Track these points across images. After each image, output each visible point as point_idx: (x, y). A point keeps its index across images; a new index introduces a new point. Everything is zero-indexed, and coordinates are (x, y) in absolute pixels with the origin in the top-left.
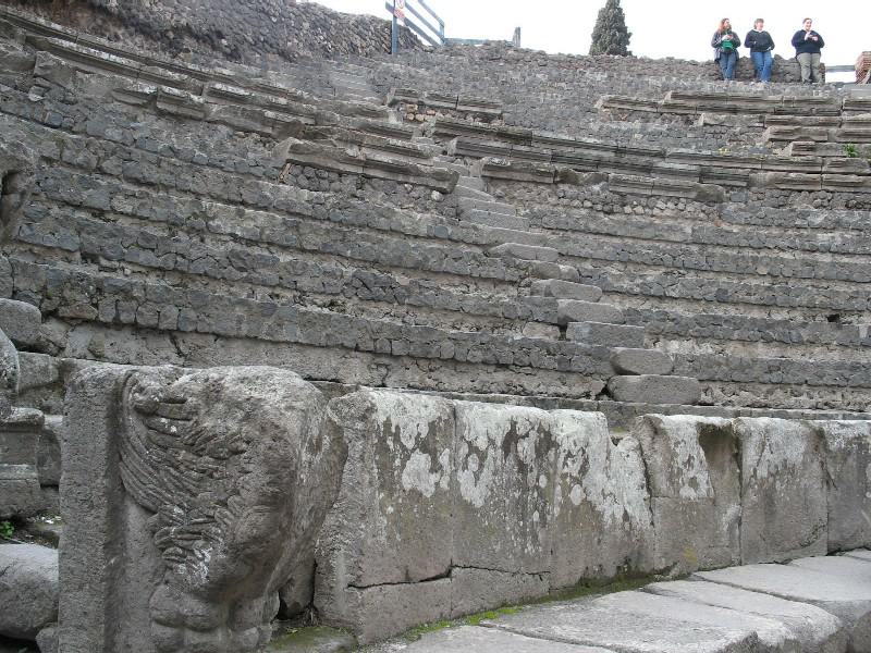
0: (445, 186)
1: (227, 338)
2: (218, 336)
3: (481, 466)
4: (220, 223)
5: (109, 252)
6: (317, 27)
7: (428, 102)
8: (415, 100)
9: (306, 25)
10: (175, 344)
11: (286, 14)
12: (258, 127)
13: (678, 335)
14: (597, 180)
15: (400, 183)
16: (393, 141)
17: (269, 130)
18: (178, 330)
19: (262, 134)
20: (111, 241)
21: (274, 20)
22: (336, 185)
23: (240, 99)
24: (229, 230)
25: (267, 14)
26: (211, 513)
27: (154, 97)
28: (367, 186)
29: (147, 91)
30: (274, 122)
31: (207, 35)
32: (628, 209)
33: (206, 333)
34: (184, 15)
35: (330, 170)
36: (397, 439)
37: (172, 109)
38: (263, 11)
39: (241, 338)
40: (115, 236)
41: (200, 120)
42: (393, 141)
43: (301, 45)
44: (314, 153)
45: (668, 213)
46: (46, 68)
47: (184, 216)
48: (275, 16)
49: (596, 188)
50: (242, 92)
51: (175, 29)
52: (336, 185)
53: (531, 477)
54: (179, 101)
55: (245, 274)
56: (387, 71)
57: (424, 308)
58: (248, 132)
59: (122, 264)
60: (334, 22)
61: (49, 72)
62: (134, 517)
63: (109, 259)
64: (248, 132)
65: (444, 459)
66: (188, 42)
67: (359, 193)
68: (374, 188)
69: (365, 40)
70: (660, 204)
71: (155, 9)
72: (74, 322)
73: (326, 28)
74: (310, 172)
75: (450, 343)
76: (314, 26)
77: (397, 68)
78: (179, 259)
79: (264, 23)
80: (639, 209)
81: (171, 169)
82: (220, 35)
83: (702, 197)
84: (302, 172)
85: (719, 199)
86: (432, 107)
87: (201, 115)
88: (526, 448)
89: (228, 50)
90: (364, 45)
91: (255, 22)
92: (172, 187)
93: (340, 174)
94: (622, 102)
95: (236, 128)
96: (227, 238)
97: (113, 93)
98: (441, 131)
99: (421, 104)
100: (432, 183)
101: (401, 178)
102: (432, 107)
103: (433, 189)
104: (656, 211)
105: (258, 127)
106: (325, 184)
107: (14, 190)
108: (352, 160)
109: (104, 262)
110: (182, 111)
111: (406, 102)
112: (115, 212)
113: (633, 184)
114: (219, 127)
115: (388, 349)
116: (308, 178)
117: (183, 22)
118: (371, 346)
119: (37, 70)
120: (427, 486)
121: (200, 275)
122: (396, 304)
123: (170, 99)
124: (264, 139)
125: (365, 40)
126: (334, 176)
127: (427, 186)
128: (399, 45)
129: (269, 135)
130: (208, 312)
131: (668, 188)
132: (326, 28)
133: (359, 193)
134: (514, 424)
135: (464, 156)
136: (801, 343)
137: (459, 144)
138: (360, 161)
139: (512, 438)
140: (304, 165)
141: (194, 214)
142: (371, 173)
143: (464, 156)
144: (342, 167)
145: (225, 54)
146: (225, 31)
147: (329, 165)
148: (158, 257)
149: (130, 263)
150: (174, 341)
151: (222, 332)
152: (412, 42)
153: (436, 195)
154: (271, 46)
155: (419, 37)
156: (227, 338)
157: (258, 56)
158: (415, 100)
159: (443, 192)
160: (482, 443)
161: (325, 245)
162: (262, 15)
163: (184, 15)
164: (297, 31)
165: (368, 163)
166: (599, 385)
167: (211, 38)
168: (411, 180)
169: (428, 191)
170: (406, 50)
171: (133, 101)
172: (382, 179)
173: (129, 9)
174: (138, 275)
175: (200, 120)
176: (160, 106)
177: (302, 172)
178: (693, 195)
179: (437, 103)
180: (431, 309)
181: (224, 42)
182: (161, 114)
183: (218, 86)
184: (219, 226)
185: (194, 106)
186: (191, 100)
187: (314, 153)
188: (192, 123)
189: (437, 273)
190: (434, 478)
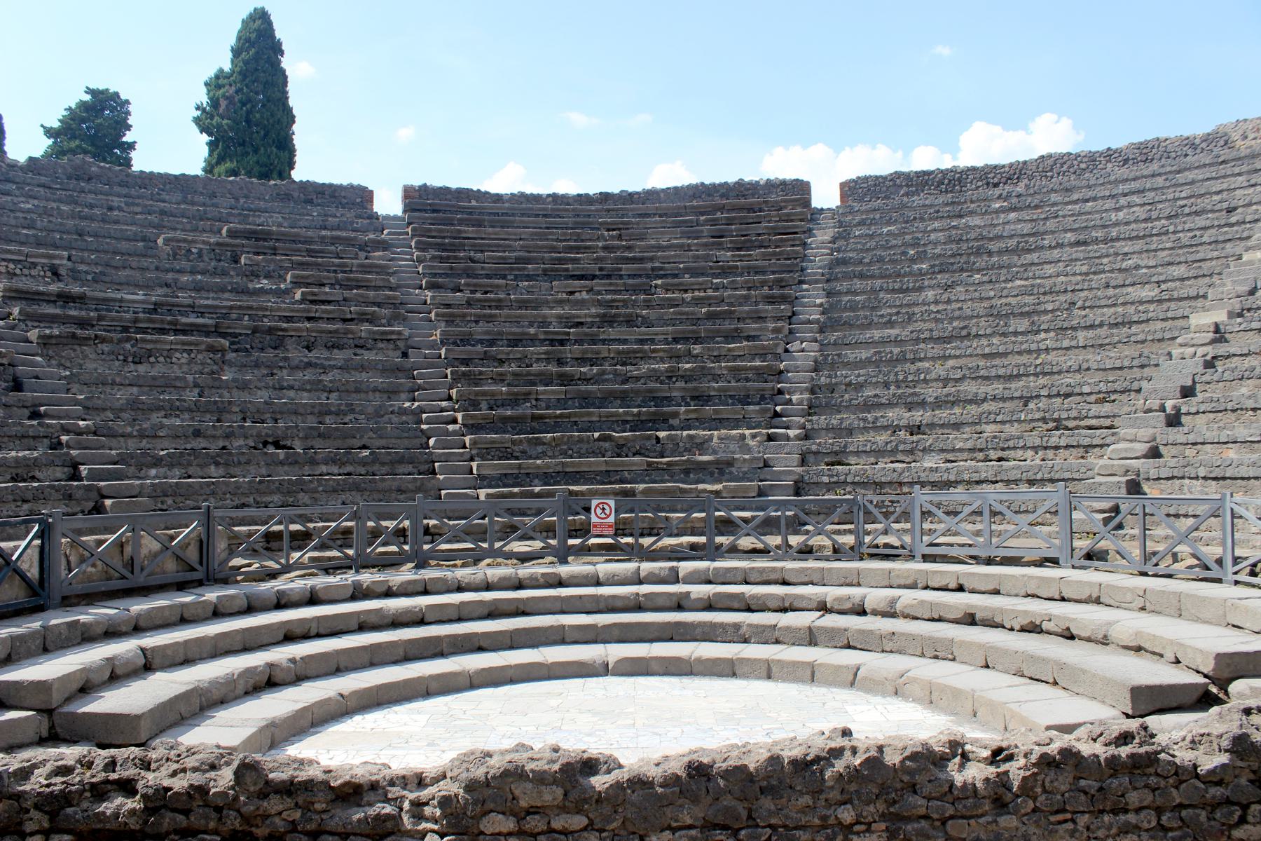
13: (155, 465)
14: (128, 340)
32: (152, 359)
45: (183, 361)
49: (128, 346)
70: (178, 355)
80: (161, 359)
83: (211, 349)
85: (223, 351)
94: (179, 241)
104: (174, 360)
113: (156, 342)
131: (184, 344)
136: (240, 463)
166: (91, 504)
178: (203, 347)
179: (9, 257)
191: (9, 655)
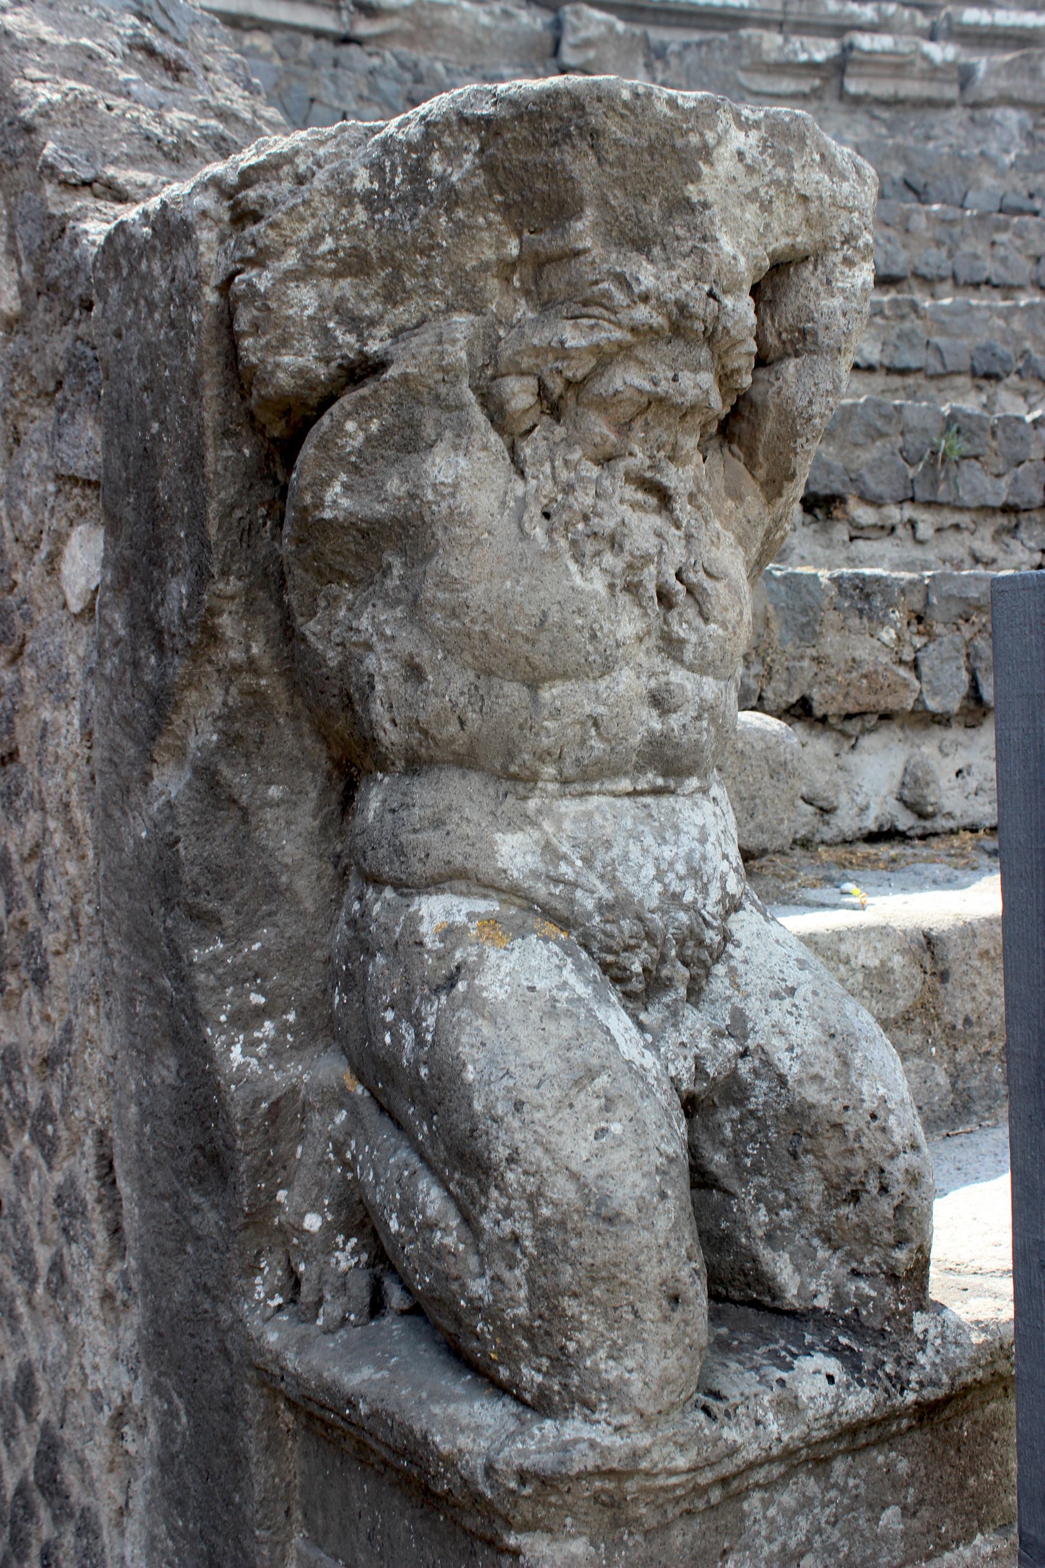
5: (874, 485)
27: (839, 66)
29: (819, 57)
37: (884, 88)
40: (882, 435)
41: (949, 105)
46: (587, 43)
54: (897, 66)
61: (591, 54)
63: (875, 502)
72: (853, 727)
87: (951, 92)
92: (942, 279)
97: (742, 77)
109: (865, 515)
110: (911, 88)
114: (998, 113)
148: (998, 476)
171: (787, 85)
174: (951, 536)
175: (949, 105)
176: (853, 86)
185: (934, 72)
186: (926, 57)
188: (932, 116)
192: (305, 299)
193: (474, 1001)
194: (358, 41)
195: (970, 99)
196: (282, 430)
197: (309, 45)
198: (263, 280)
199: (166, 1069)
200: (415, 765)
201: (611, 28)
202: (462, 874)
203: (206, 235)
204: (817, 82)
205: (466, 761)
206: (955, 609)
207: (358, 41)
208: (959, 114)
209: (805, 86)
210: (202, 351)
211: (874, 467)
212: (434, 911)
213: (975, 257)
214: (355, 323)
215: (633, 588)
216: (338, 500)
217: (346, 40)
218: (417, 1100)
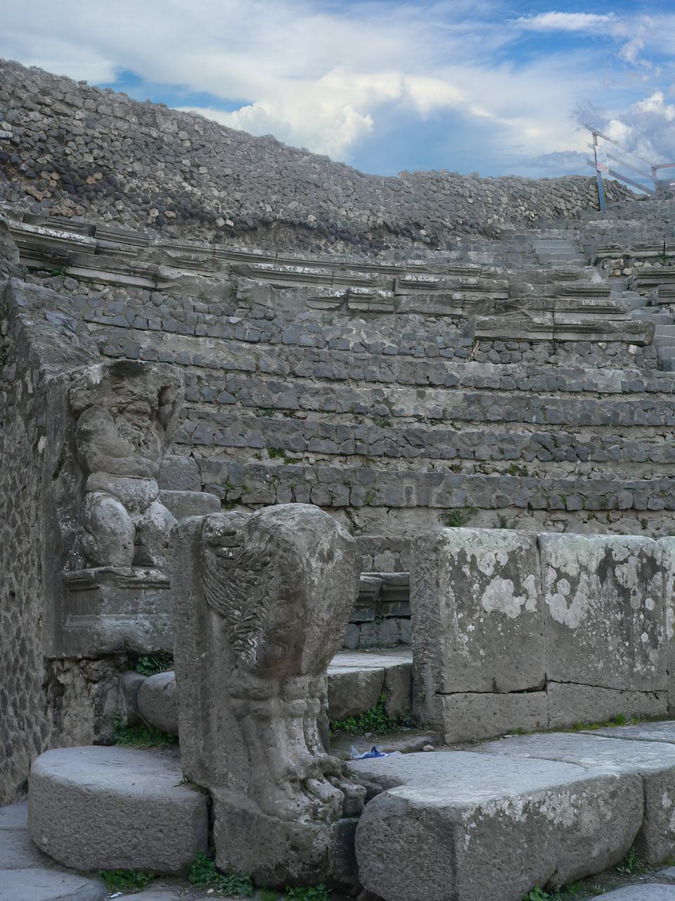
0: (642, 338)
1: (399, 508)
2: (390, 507)
3: (573, 591)
4: (403, 407)
5: (293, 446)
6: (515, 199)
7: (633, 254)
8: (619, 254)
9: (505, 200)
10: (351, 518)
11: (481, 193)
12: (448, 310)
15: (593, 342)
16: (586, 302)
17: (459, 312)
18: (351, 505)
19: (453, 316)
20: (293, 436)
21: (471, 201)
22: (529, 354)
23: (432, 286)
24: (412, 413)
25: (463, 196)
26: (255, 611)
27: (346, 299)
28: (559, 350)
29: (338, 294)
30: (463, 303)
31: (405, 229)
33: (380, 506)
34: (380, 214)
35: (519, 340)
36: (473, 565)
37: (364, 307)
38: (458, 194)
39: (412, 508)
41: (391, 313)
42: (586, 302)
43: (502, 220)
44: (502, 327)
47: (368, 405)
48: (470, 197)
50: (432, 279)
51: (373, 230)
52: (529, 354)
53: (635, 602)
54: (368, 299)
55: (423, 450)
56: (594, 229)
57: (609, 463)
58: (438, 316)
59: (307, 454)
60: (533, 190)
61: (249, 294)
62: (215, 622)
63: (294, 452)
64: (438, 316)
65: (529, 582)
66: (387, 239)
67: (552, 359)
68: (567, 351)
69: (569, 201)
71: (352, 215)
73: (525, 198)
74: (501, 346)
75: (626, 493)
76: (513, 198)
77: (604, 224)
78: (359, 443)
79: (460, 206)
81: (359, 363)
82: (418, 226)
84: (492, 347)
86: (638, 259)
87: (391, 308)
88: (627, 573)
89: (428, 240)
90: (569, 206)
91: (452, 206)
92: (361, 380)
93: (531, 343)
95: (430, 315)
96: (412, 420)
97: (308, 303)
98: (644, 282)
99: (627, 257)
100: (628, 337)
101: (593, 337)
102: (638, 259)
103: (629, 343)
105: (448, 310)
106: (517, 354)
107: (167, 402)
108: (541, 328)
109: (289, 454)
110: (373, 307)
111: (610, 257)
112: (305, 410)
114: (411, 316)
115: (561, 506)
116: (499, 352)
117: (380, 221)
118: (544, 504)
119: (239, 296)
120: (513, 607)
121: (380, 456)
122: (579, 462)
123: (360, 298)
124: (455, 321)
125: (569, 201)
126: (525, 346)
127: (623, 341)
128: (608, 200)
129: (460, 317)
130: (377, 486)
132: (525, 198)
133: (552, 359)
134: (609, 552)
135: (668, 304)
137: (662, 293)
138: (549, 327)
139: (607, 565)
140: (493, 340)
141: (378, 402)
142: (563, 337)
143: (668, 304)
144: (532, 336)
145: (425, 243)
146: (422, 221)
147: (519, 336)
149: (313, 452)
150: (349, 515)
151: (392, 504)
152: (619, 192)
153: (633, 349)
154: (471, 226)
155: (629, 187)
156: (399, 508)
157: (458, 239)
158: (619, 254)
159: (640, 344)
160: (572, 570)
161: (509, 414)
162: (459, 199)
163: (380, 214)
164: (495, 207)
165: (558, 328)
167: (409, 231)
168: (605, 337)
169: (625, 346)
170: (617, 204)
171: (325, 306)
172: (577, 342)
173: (328, 220)
174: (322, 463)
175: (391, 313)
176: (352, 306)
177: (492, 347)
180: (616, 462)
181: (423, 232)
182: (353, 313)
183: (408, 278)
184: (402, 410)
185: (383, 301)
186: (380, 295)
187: (502, 327)
188: (384, 317)
189: (629, 426)
190: (518, 601)
191: (640, 840)
192: (81, 394)
193: (99, 505)
194: (160, 290)
195: (398, 311)
196: (76, 414)
197: (141, 293)
198: (74, 391)
199: (52, 535)
200: (95, 471)
201: (257, 285)
202: (101, 489)
203: (66, 382)
204: (338, 305)
205: (104, 469)
206: (287, 475)
207: (160, 290)
208: (393, 317)
209: (333, 306)
210: (64, 404)
211: (296, 440)
212: (97, 494)
213: (374, 372)
214: (89, 398)
215: (133, 442)
216: (85, 427)
217: (155, 290)
218: (92, 526)
